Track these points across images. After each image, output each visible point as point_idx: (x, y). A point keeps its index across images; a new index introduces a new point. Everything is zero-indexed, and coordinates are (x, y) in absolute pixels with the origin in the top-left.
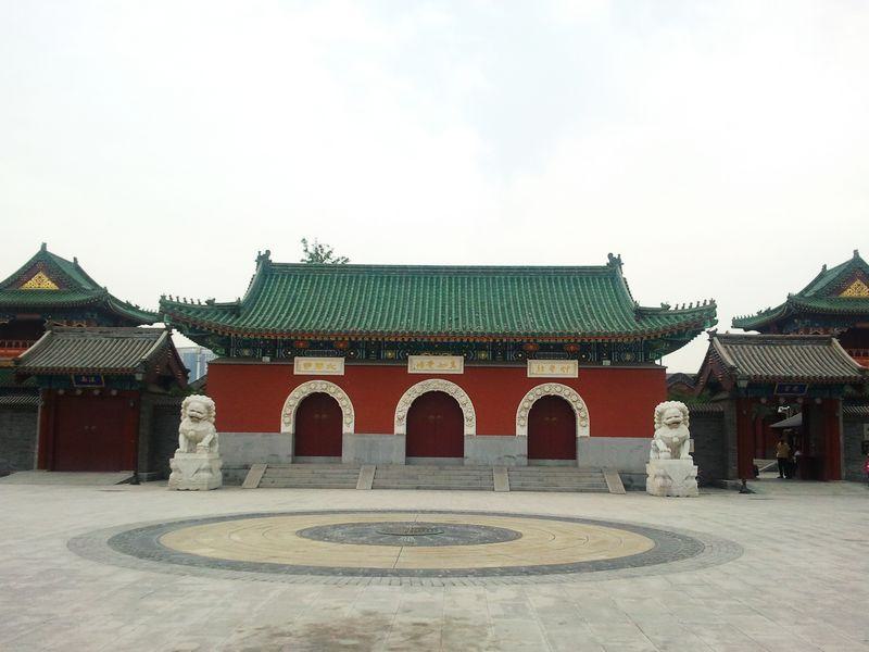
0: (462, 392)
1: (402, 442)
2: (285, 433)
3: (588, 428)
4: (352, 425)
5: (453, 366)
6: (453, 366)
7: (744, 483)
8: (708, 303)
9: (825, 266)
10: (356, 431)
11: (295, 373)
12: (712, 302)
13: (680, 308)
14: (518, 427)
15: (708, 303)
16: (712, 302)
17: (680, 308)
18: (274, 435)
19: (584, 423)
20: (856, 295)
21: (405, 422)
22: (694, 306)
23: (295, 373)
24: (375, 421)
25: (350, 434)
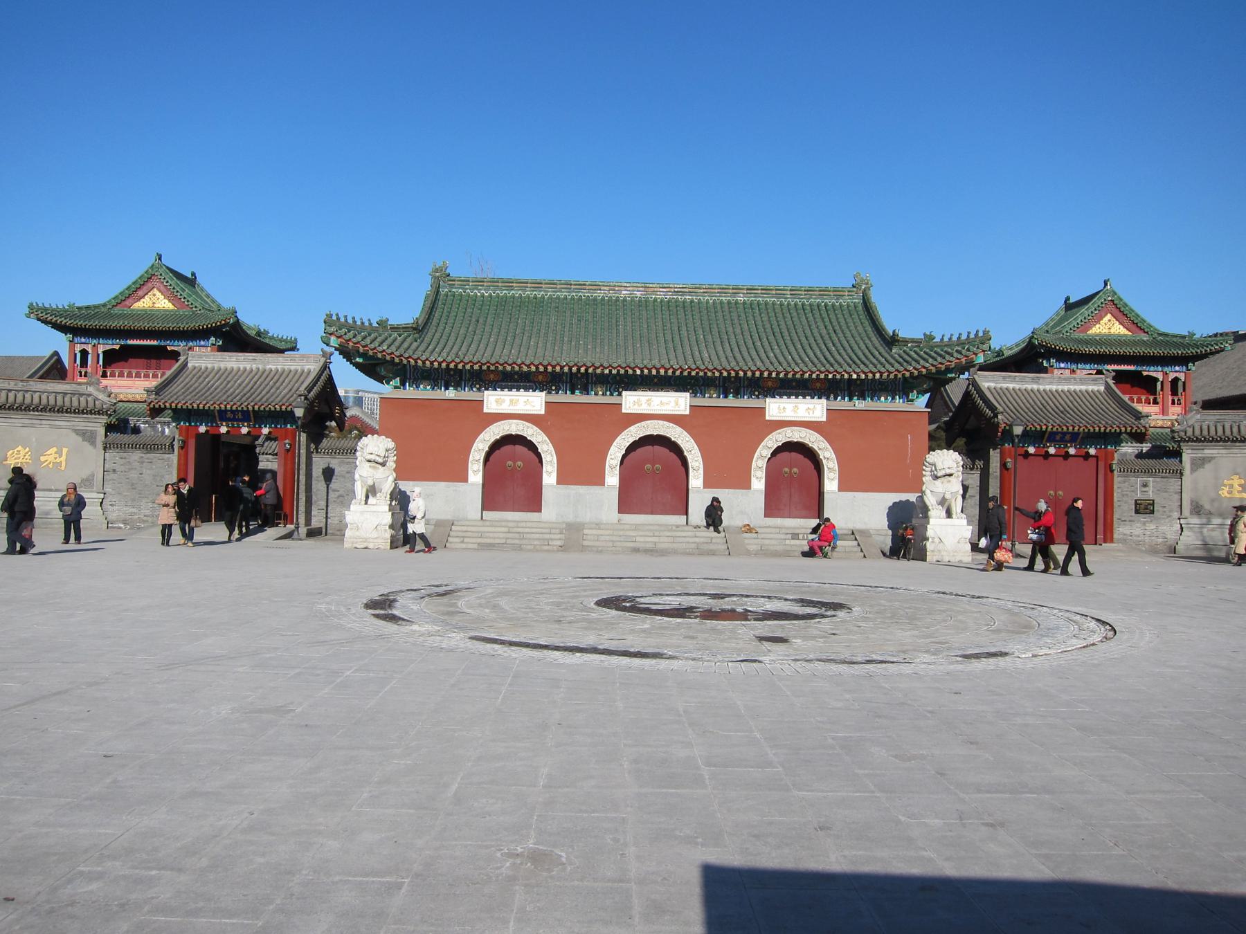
0: (688, 437)
1: (615, 495)
2: (473, 484)
3: (836, 481)
4: (554, 475)
5: (677, 404)
6: (677, 404)
7: (1013, 545)
8: (981, 334)
9: (1068, 299)
10: (559, 482)
11: (485, 410)
12: (986, 332)
13: (946, 339)
14: (753, 480)
15: (981, 334)
16: (986, 332)
17: (946, 339)
18: (460, 486)
19: (832, 475)
20: (1105, 331)
21: (617, 472)
22: (964, 337)
23: (485, 410)
24: (581, 470)
25: (552, 486)
